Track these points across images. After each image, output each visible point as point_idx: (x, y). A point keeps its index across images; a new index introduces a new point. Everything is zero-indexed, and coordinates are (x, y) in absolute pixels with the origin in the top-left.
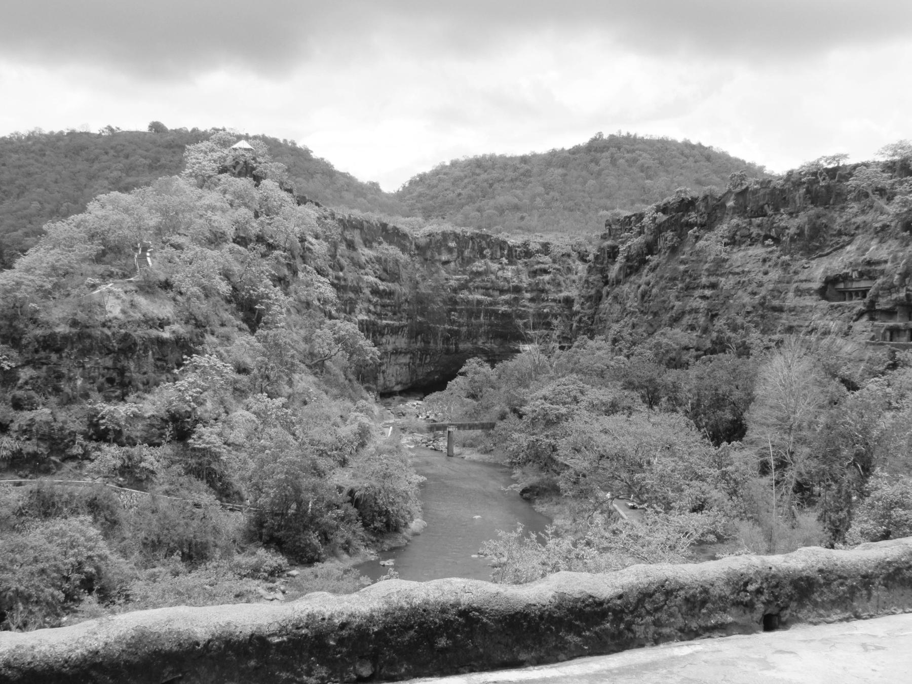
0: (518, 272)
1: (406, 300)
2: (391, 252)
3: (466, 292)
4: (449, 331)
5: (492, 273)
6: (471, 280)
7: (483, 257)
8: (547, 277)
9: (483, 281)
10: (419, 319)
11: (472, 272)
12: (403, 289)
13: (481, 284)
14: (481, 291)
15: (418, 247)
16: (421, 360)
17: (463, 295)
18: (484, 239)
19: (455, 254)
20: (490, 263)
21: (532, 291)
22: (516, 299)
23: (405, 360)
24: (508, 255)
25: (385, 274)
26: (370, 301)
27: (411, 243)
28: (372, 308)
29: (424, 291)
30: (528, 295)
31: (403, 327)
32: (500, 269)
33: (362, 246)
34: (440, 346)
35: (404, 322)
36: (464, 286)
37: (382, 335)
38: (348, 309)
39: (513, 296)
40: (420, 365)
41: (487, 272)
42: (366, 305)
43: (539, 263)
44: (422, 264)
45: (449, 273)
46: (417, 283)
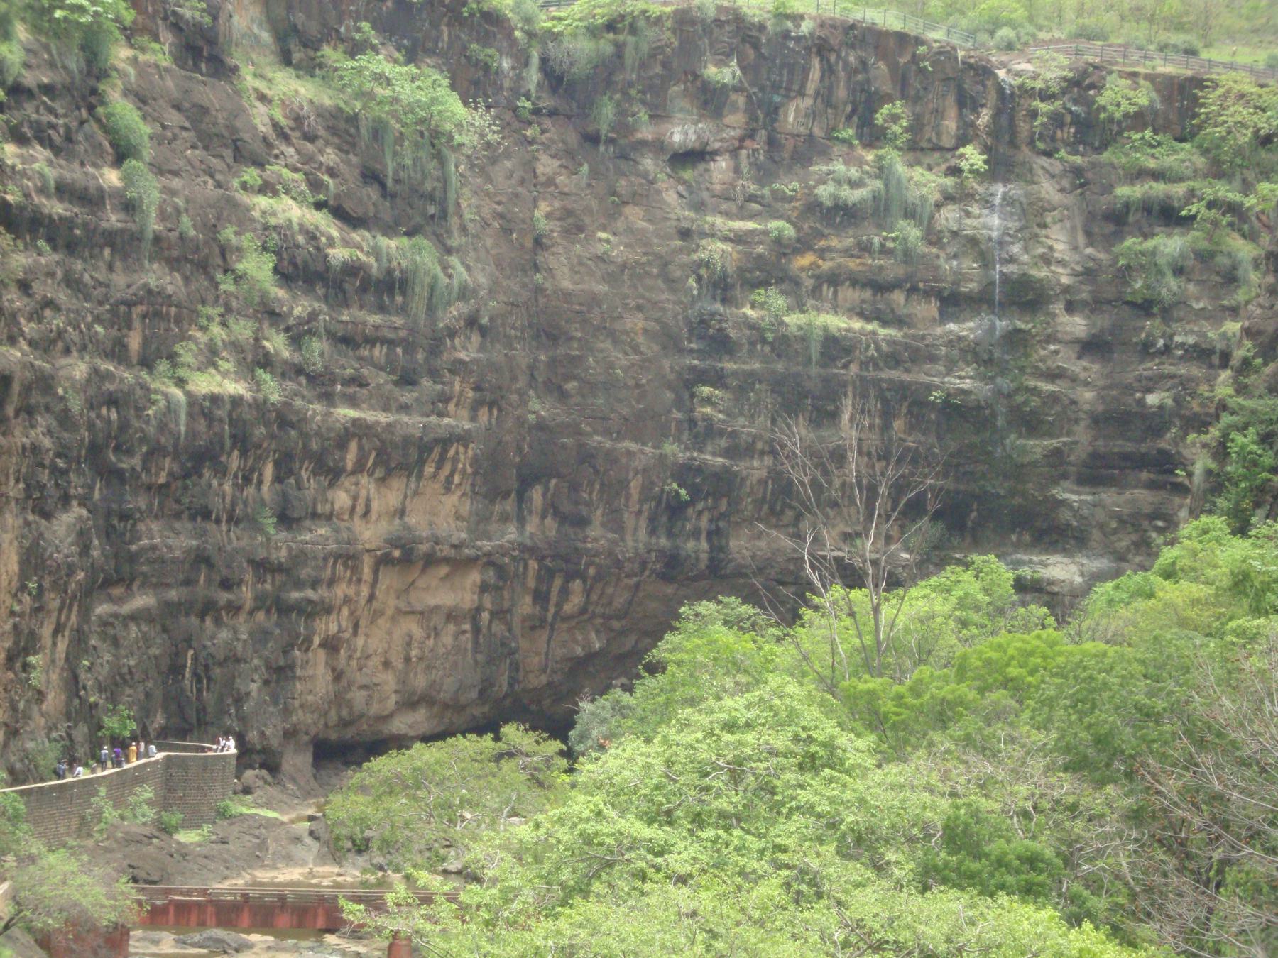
0: (1032, 216)
1: (472, 322)
2: (406, 92)
3: (778, 301)
4: (684, 473)
5: (910, 213)
6: (803, 244)
7: (874, 136)
8: (1171, 244)
9: (865, 248)
10: (539, 408)
11: (813, 207)
12: (453, 271)
13: (852, 264)
14: (850, 295)
15: (554, 78)
16: (540, 597)
17: (766, 308)
18: (882, 54)
19: (735, 121)
20: (901, 169)
21: (1095, 305)
22: (1015, 340)
23: (459, 593)
24: (995, 131)
25: (372, 193)
26: (271, 314)
27: (523, 61)
28: (277, 343)
29: (566, 284)
30: (1077, 325)
31: (446, 442)
32: (948, 198)
33: (267, 61)
34: (637, 538)
35: (457, 420)
36: (766, 270)
37: (334, 474)
38: (134, 342)
39: (1002, 325)
40: (535, 625)
41: (881, 209)
42: (243, 329)
43: (1141, 174)
44: (570, 157)
45: (699, 207)
46: (539, 243)
